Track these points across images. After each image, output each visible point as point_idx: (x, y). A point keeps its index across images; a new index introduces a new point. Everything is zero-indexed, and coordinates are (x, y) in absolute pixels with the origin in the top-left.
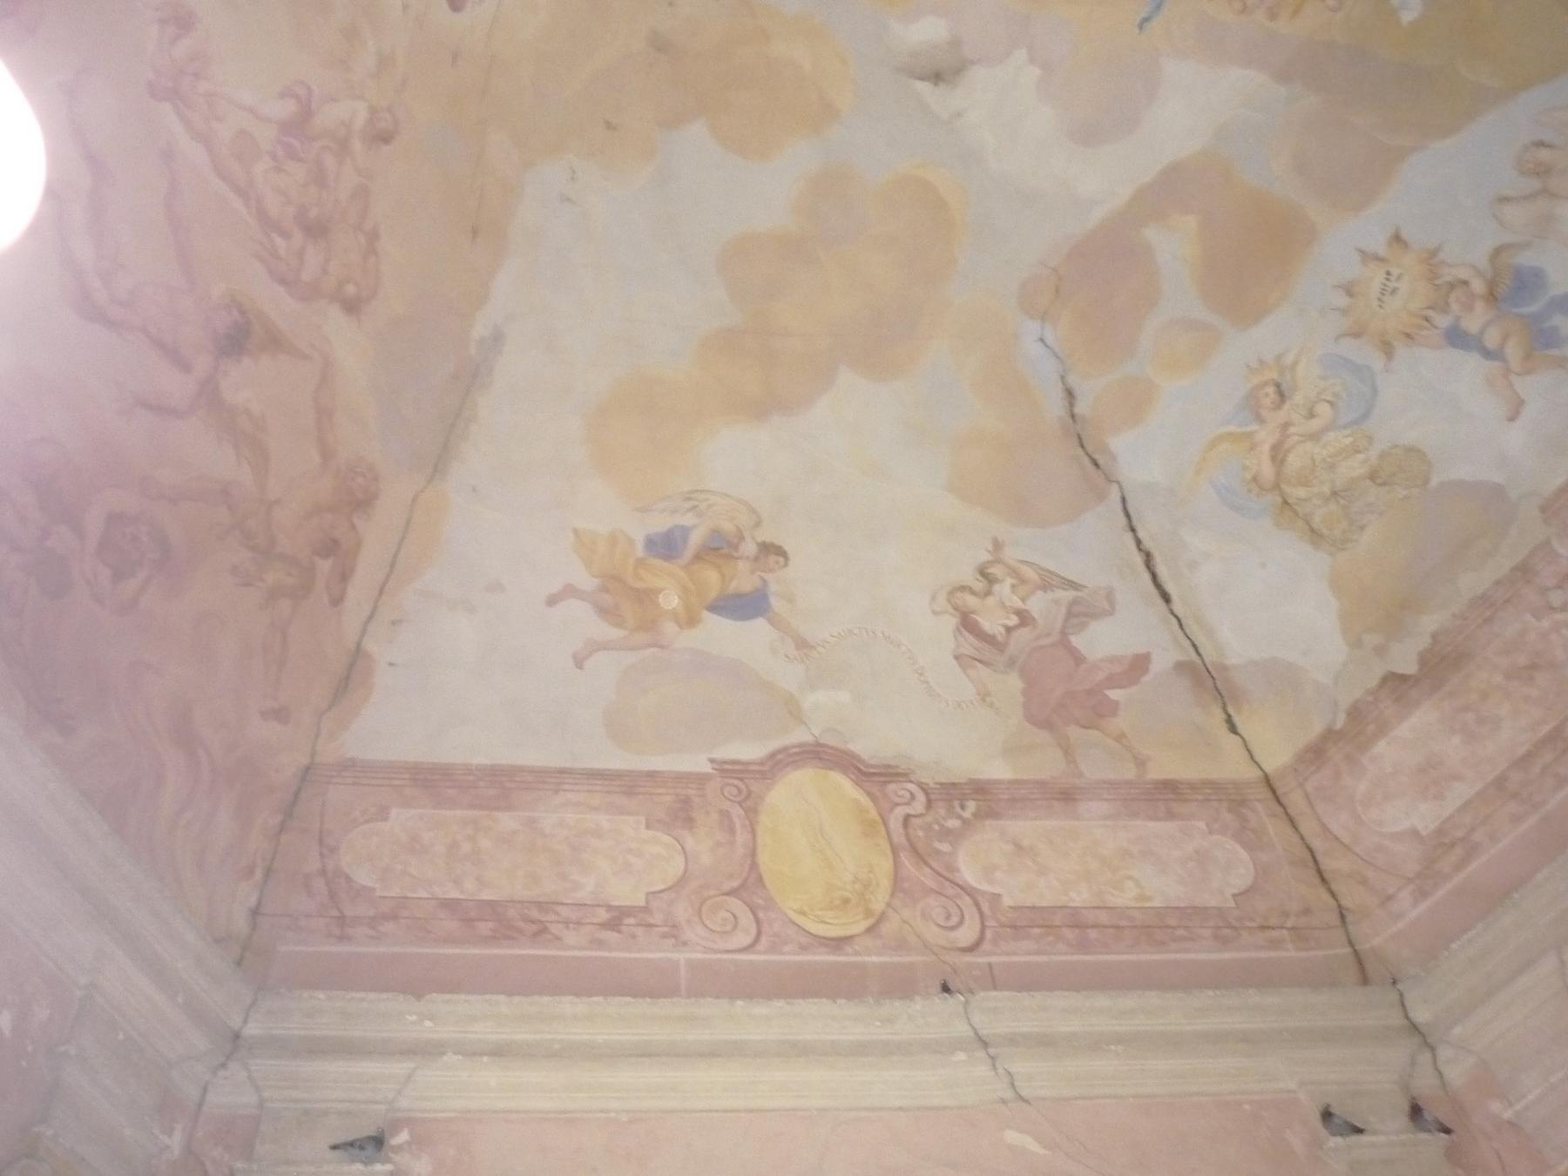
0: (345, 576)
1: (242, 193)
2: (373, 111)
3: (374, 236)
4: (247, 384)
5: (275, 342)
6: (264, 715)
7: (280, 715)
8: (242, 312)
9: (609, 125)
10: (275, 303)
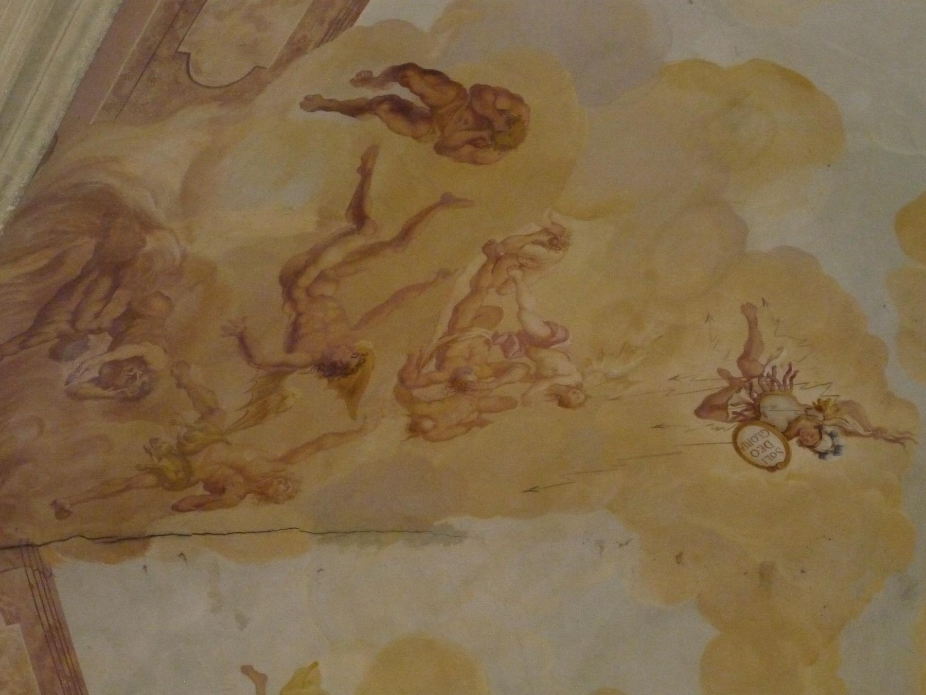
0: (200, 506)
1: (452, 327)
2: (579, 387)
3: (482, 424)
4: (307, 392)
5: (352, 394)
6: (54, 504)
7: (61, 512)
8: (359, 365)
9: (679, 557)
10: (381, 381)
